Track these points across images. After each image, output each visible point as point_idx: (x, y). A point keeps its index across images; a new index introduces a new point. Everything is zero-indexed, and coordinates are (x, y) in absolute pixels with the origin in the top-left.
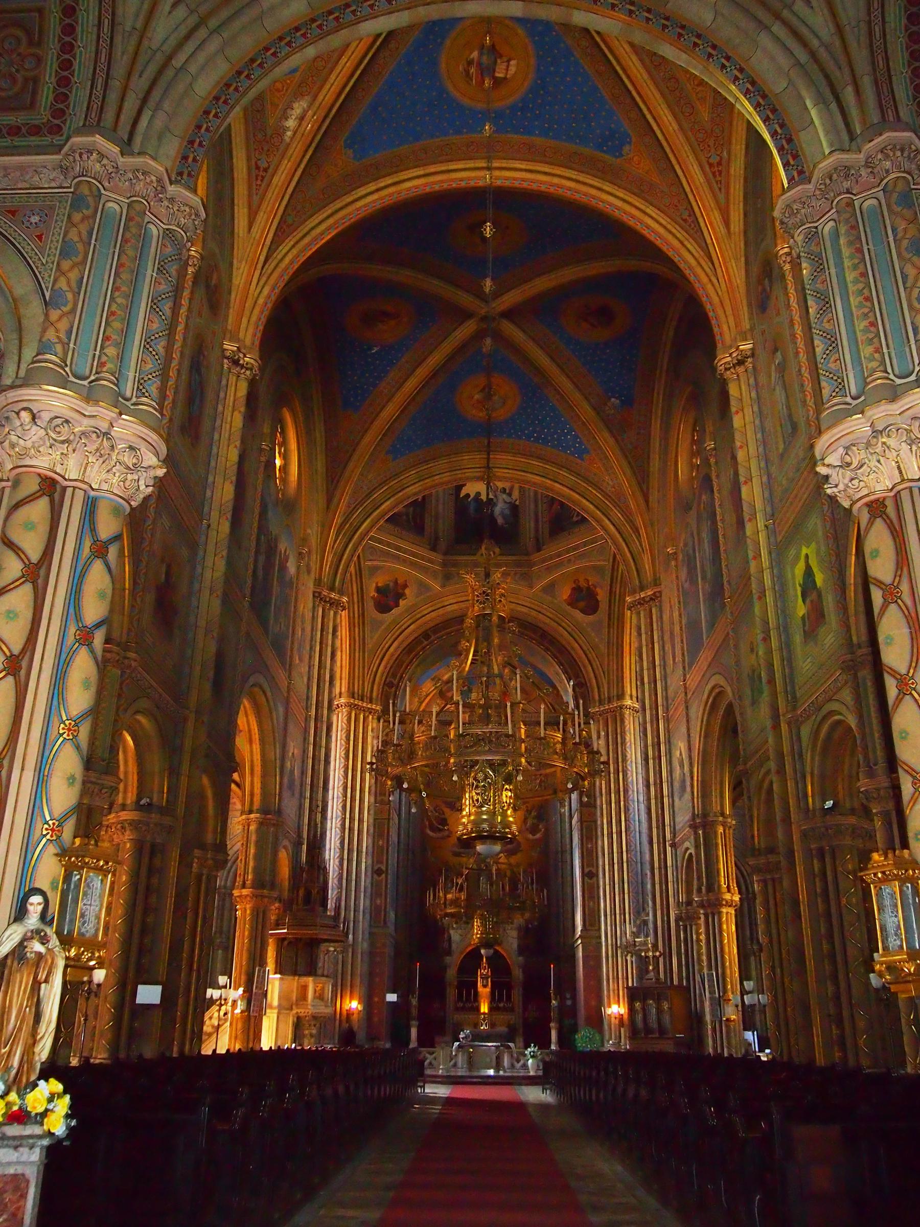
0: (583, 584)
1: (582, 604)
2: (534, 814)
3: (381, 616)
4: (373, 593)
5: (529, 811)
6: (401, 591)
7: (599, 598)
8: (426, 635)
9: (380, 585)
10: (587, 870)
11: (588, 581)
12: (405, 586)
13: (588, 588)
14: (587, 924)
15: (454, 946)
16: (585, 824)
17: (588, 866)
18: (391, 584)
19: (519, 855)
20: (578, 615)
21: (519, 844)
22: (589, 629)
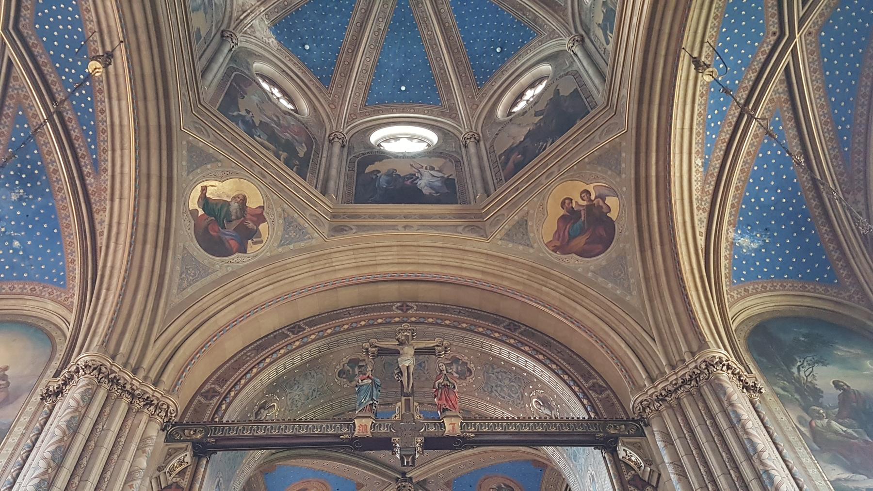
0: (579, 202)
1: (581, 241)
3: (206, 258)
4: (193, 203)
6: (251, 225)
7: (613, 215)
8: (295, 328)
9: (208, 195)
11: (588, 192)
12: (260, 217)
13: (590, 207)
18: (234, 206)
20: (574, 261)
22: (600, 279)
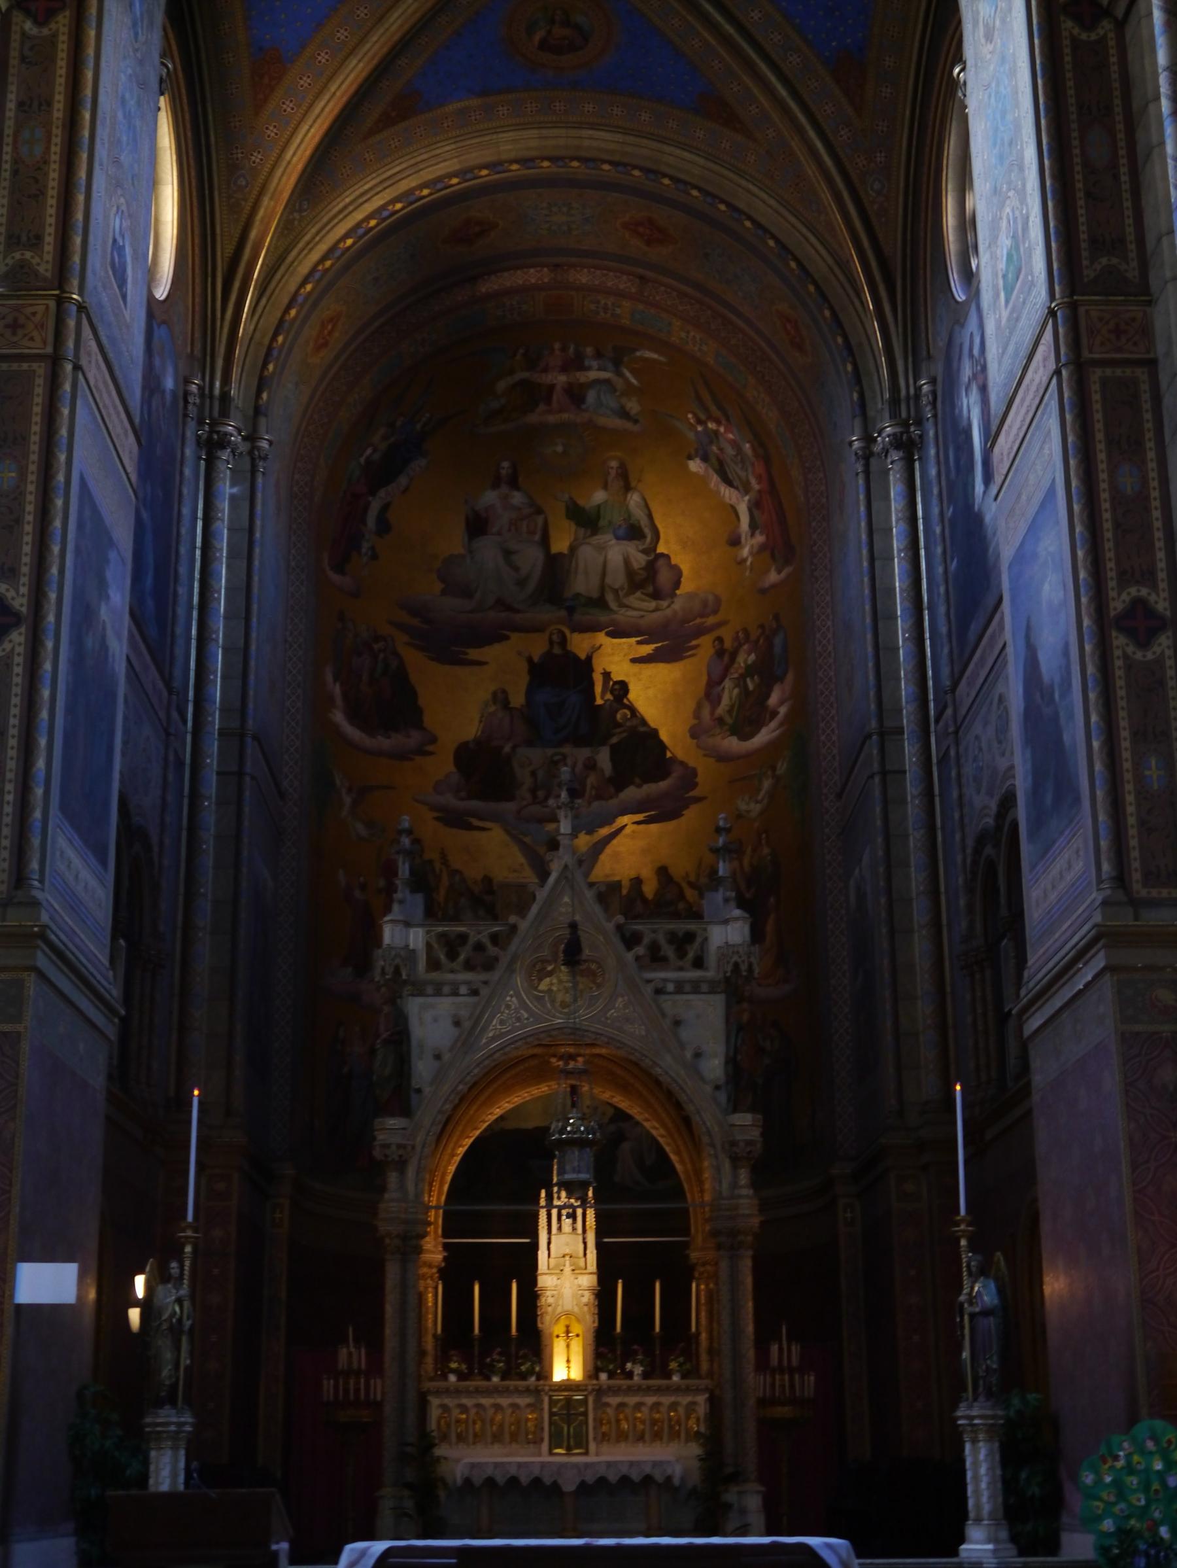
2: (746, 658)
5: (724, 655)
10: (1118, 604)
14: (1137, 876)
15: (422, 1069)
16: (1096, 375)
17: (1125, 578)
19: (691, 814)
21: (690, 777)
